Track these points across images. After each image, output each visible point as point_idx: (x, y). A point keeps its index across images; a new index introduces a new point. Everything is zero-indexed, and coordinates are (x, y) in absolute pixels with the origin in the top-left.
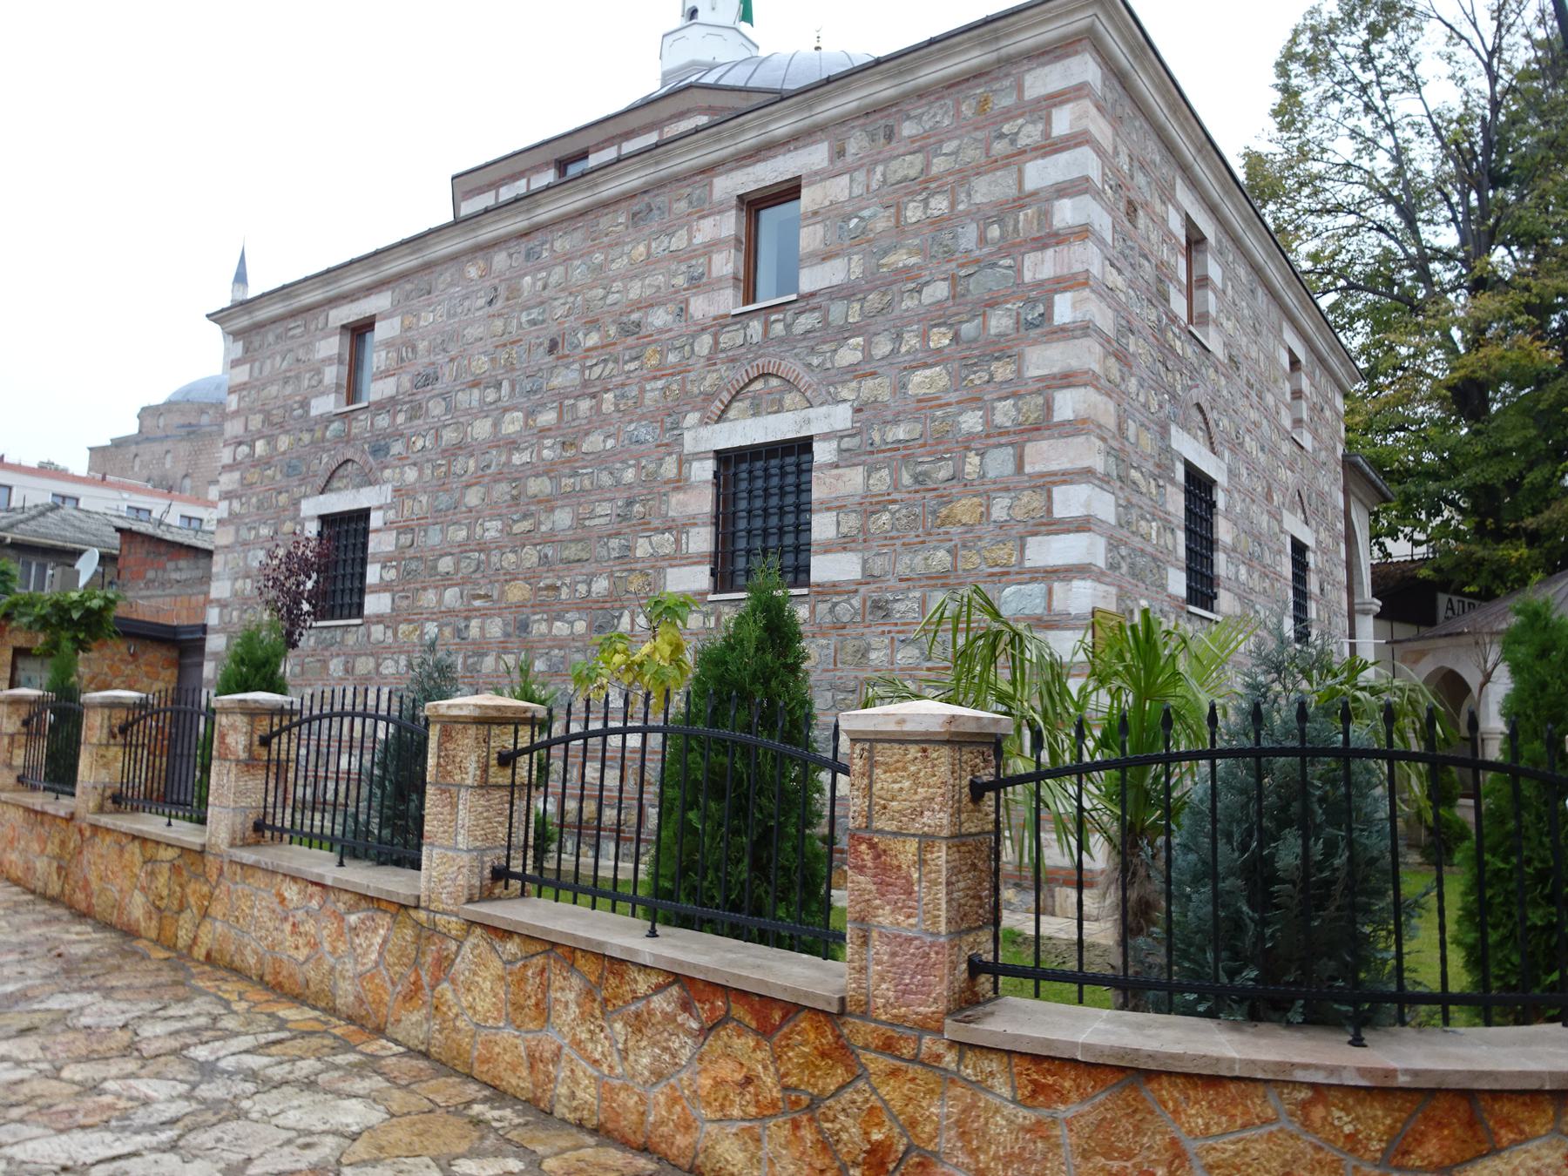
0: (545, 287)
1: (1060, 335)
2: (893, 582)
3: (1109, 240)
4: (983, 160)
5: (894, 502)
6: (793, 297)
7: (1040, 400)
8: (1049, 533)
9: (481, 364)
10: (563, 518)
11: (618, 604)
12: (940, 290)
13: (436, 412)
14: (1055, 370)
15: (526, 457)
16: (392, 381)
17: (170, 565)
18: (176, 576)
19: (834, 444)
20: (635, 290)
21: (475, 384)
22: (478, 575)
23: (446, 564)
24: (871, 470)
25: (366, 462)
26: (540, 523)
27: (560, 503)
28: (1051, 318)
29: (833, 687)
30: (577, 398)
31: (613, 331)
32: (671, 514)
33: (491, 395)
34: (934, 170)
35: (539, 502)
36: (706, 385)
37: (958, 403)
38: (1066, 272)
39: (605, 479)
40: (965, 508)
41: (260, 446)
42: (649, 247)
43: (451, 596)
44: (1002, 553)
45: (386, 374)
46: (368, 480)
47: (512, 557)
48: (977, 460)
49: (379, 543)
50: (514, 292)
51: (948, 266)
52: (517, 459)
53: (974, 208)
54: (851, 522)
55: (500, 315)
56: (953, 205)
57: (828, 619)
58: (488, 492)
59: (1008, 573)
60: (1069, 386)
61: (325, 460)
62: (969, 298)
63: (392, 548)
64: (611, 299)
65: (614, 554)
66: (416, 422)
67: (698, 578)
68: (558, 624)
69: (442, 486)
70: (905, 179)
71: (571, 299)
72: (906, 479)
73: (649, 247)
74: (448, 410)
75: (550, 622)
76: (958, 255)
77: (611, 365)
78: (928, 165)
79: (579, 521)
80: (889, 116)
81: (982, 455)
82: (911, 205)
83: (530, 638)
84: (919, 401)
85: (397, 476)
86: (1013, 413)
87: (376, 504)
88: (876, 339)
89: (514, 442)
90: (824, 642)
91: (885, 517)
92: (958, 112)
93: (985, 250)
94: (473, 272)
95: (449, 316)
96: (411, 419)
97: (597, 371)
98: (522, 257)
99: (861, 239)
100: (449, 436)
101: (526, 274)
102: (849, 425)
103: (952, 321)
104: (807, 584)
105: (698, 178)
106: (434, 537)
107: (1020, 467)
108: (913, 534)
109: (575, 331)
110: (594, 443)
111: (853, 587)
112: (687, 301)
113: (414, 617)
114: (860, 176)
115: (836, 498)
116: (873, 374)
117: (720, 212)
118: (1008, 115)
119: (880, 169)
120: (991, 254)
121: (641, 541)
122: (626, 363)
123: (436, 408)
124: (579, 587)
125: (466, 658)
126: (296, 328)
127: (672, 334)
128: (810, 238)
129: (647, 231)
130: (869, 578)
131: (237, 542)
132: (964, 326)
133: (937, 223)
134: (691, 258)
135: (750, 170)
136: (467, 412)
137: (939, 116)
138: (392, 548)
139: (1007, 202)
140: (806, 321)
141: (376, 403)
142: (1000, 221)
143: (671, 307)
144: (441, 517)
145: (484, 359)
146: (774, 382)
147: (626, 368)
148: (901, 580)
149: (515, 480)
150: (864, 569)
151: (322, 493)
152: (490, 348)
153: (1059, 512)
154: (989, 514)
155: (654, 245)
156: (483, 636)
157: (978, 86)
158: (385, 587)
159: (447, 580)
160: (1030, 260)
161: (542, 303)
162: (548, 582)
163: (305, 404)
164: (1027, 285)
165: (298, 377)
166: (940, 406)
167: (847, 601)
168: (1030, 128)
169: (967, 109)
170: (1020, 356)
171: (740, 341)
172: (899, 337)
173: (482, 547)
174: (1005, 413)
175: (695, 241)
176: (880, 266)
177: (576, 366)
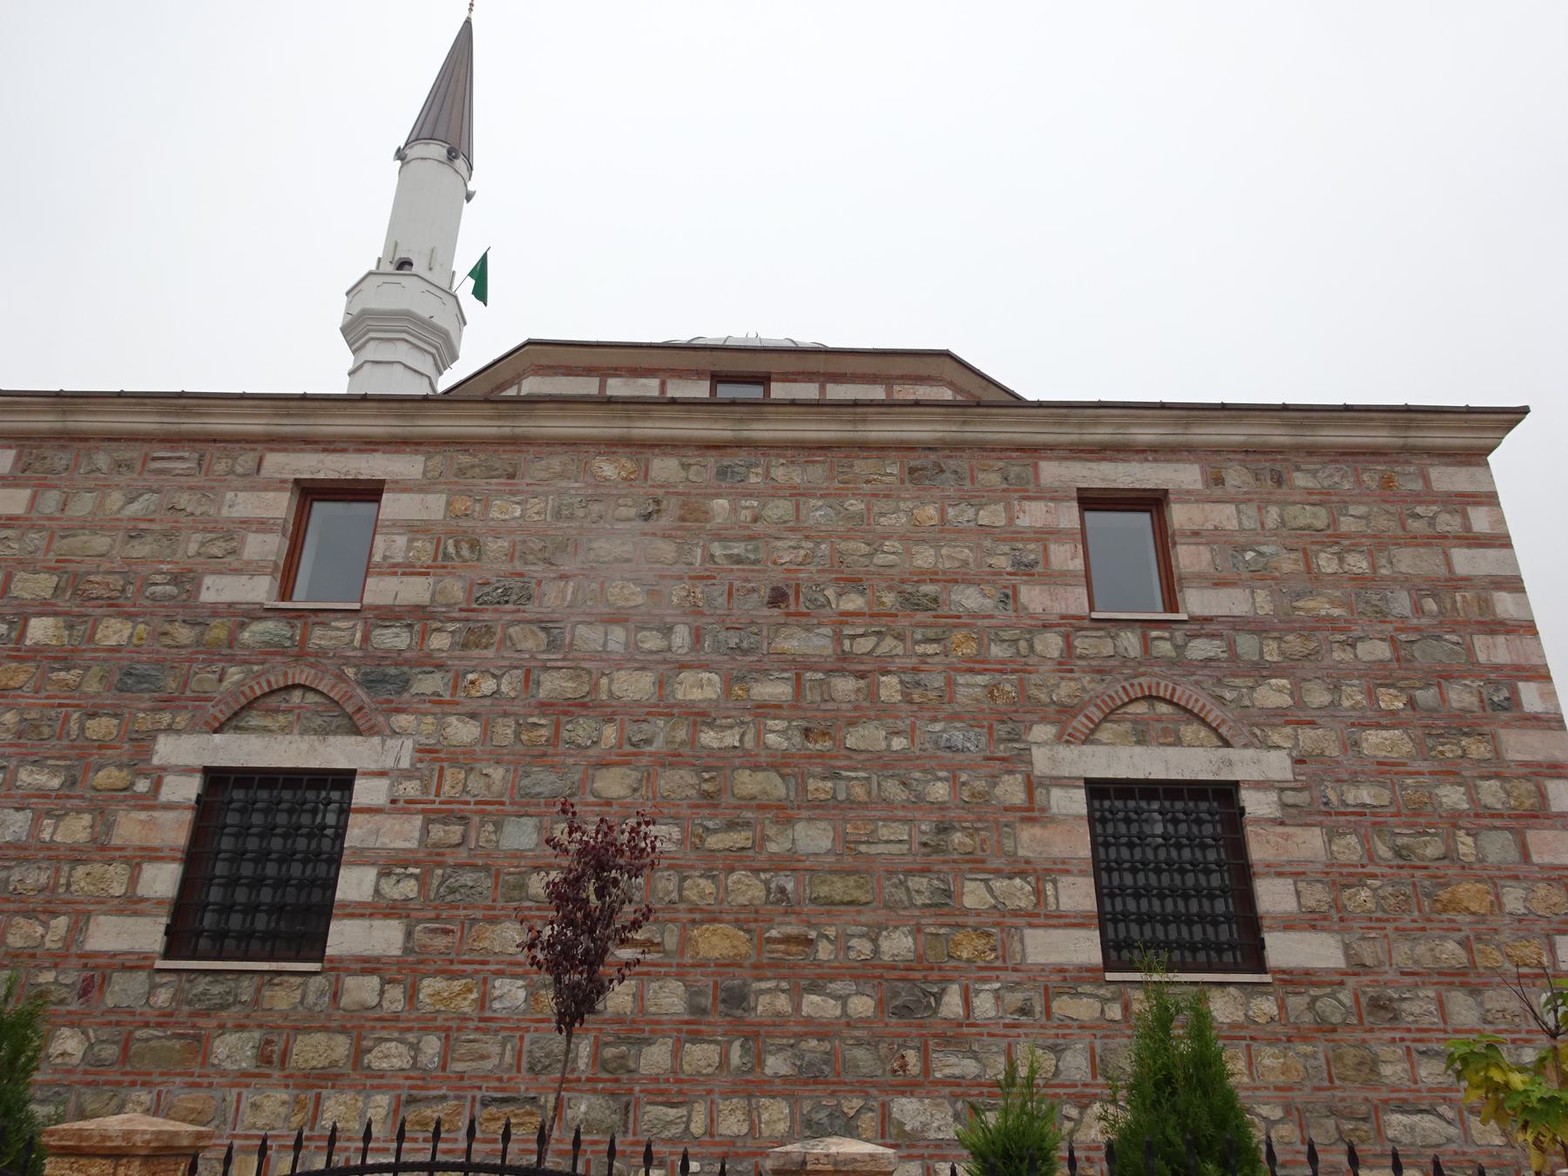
0: (755, 520)
5: (1373, 876)
9: (629, 595)
10: (814, 838)
11: (935, 975)
13: (529, 644)
14: (1539, 757)
15: (731, 738)
19: (1273, 796)
20: (925, 558)
21: (616, 618)
24: (1332, 834)
26: (766, 838)
27: (805, 813)
28: (1519, 704)
29: (1332, 1112)
30: (829, 672)
31: (889, 599)
32: (1021, 852)
33: (652, 641)
35: (762, 807)
37: (1431, 773)
38: (1523, 661)
39: (893, 790)
42: (943, 512)
47: (707, 886)
48: (1469, 840)
51: (1384, 626)
52: (709, 738)
53: (1401, 578)
54: (1317, 896)
56: (1374, 567)
58: (649, 778)
63: (413, 844)
64: (880, 559)
67: (1086, 948)
68: (815, 998)
70: (1309, 527)
72: (1383, 851)
73: (943, 512)
74: (552, 645)
75: (796, 994)
76: (1390, 618)
79: (847, 844)
81: (1473, 834)
82: (1322, 555)
83: (751, 1017)
84: (1379, 763)
86: (1502, 795)
87: (373, 767)
88: (1308, 685)
89: (703, 714)
90: (1309, 1049)
91: (1364, 894)
93: (1424, 621)
95: (558, 515)
96: (465, 646)
97: (864, 645)
100: (553, 685)
101: (718, 496)
103: (1401, 684)
105: (1014, 454)
108: (1406, 917)
111: (1337, 978)
112: (1014, 586)
114: (1250, 510)
115: (1290, 863)
116: (1311, 723)
117: (1052, 499)
118: (1418, 498)
119: (1274, 511)
120: (1434, 627)
121: (969, 886)
122: (917, 642)
124: (854, 942)
125: (597, 1046)
126: (183, 462)
127: (993, 622)
129: (937, 493)
130: (1357, 967)
133: (1357, 578)
134: (1013, 539)
135: (1093, 465)
136: (593, 656)
137: (1339, 478)
140: (1200, 649)
141: (378, 607)
146: (1163, 708)
147: (920, 649)
148: (1403, 973)
149: (707, 769)
150: (1347, 956)
151: (216, 731)
154: (1501, 905)
155: (951, 512)
156: (642, 1010)
160: (1480, 642)
161: (751, 538)
163: (187, 579)
165: (170, 535)
166: (1410, 774)
167: (1332, 995)
169: (1370, 480)
172: (1336, 688)
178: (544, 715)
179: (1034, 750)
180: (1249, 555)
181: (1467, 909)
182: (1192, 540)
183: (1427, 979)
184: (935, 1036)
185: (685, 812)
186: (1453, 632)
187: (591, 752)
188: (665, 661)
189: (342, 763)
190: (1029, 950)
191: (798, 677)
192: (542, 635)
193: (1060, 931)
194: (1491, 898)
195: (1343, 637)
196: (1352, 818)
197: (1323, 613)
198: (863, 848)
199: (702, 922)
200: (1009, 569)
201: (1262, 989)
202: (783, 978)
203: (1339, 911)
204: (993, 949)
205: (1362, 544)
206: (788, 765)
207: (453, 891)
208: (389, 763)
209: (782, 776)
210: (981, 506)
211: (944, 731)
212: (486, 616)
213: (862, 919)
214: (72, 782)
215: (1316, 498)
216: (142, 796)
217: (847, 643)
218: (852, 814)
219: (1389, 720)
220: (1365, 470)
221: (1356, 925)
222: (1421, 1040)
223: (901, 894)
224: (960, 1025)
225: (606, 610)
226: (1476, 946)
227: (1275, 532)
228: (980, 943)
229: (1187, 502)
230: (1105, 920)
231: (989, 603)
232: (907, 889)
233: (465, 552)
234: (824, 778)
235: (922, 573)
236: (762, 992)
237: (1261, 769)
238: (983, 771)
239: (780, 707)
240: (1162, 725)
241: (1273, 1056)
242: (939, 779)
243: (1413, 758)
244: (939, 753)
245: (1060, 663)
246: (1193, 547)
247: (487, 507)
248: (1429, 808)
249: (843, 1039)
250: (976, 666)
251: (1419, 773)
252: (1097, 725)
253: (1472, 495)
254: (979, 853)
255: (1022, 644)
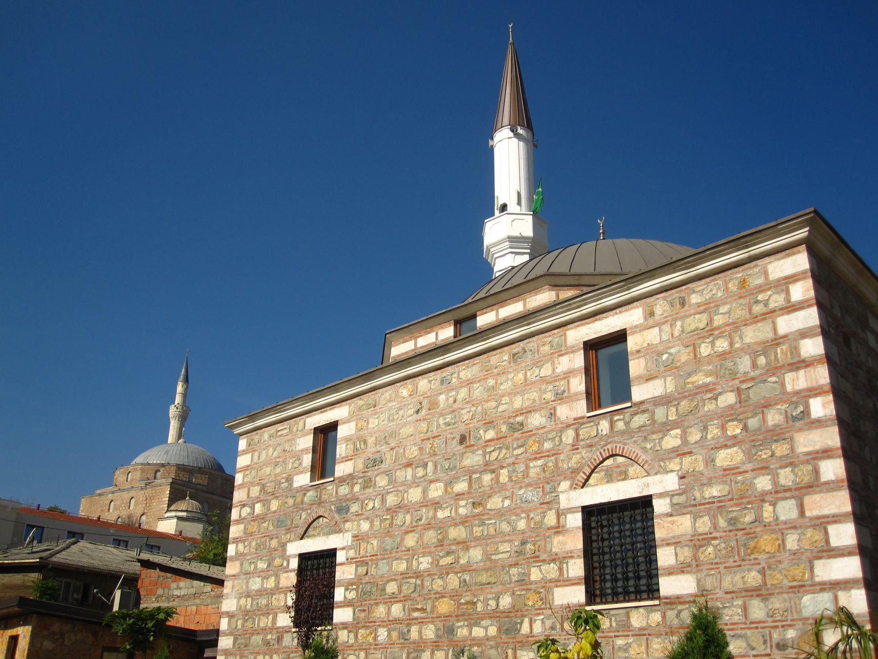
0: (455, 401)
1: (817, 424)
2: (721, 594)
3: (838, 361)
4: (748, 316)
5: (715, 538)
6: (629, 404)
7: (810, 467)
8: (830, 557)
9: (412, 452)
10: (476, 554)
12: (729, 399)
14: (817, 447)
15: (447, 513)
16: (350, 463)
17: (174, 585)
18: (176, 593)
19: (668, 500)
21: (409, 465)
22: (415, 595)
23: (392, 588)
25: (333, 518)
26: (459, 558)
27: (473, 544)
28: (809, 414)
30: (481, 472)
31: (504, 428)
32: (554, 550)
33: (420, 472)
34: (716, 324)
35: (458, 543)
36: (573, 463)
37: (753, 470)
38: (814, 384)
40: (766, 542)
41: (258, 508)
43: (397, 610)
44: (797, 572)
45: (347, 459)
46: (336, 529)
47: (440, 582)
48: (771, 508)
49: (344, 573)
50: (434, 404)
51: (733, 382)
52: (441, 514)
54: (686, 553)
55: (424, 420)
56: (731, 344)
57: (676, 622)
58: (421, 536)
59: (803, 586)
60: (829, 457)
61: (304, 517)
62: (751, 402)
63: (353, 576)
65: (515, 579)
66: (367, 491)
69: (388, 533)
71: (473, 409)
72: (722, 523)
73: (526, 374)
75: (470, 627)
76: (739, 375)
77: (504, 451)
78: (711, 321)
79: (487, 556)
80: (681, 291)
81: (774, 505)
82: (703, 345)
83: (455, 638)
84: (725, 470)
85: (355, 527)
86: (792, 477)
88: (690, 430)
89: (438, 503)
91: (710, 549)
92: (727, 288)
93: (757, 372)
94: (404, 391)
95: (389, 421)
96: (364, 488)
97: (495, 455)
98: (438, 383)
99: (671, 367)
100: (391, 500)
101: (441, 393)
102: (677, 487)
103: (741, 417)
104: (659, 598)
105: (556, 331)
106: (383, 568)
107: (802, 513)
108: (731, 560)
109: (478, 429)
110: (495, 503)
112: (555, 408)
113: (371, 624)
114: (666, 328)
115: (673, 537)
116: (690, 453)
117: (573, 352)
118: (760, 289)
119: (679, 323)
120: (762, 375)
121: (533, 570)
122: (515, 449)
123: (382, 481)
124: (490, 602)
125: (408, 654)
128: (636, 367)
129: (523, 365)
131: (241, 572)
132: (749, 421)
133: (723, 355)
134: (555, 381)
135: (591, 326)
136: (403, 484)
138: (353, 576)
139: (768, 342)
140: (639, 420)
141: (339, 478)
142: (765, 353)
143: (543, 412)
144: (385, 554)
145: (414, 448)
146: (620, 460)
147: (515, 452)
148: (727, 593)
149: (440, 528)
150: (698, 585)
151: (302, 539)
152: (419, 441)
153: (834, 542)
155: (529, 373)
156: (421, 637)
157: (739, 272)
158: (347, 603)
159: (394, 599)
160: (789, 377)
161: (453, 411)
162: (468, 599)
163: (290, 480)
164: (789, 394)
166: (740, 473)
168: (775, 297)
169: (733, 286)
170: (792, 439)
171: (594, 433)
172: (705, 428)
173: (418, 575)
174: (786, 477)
175: (557, 370)
176: (686, 384)
177: (480, 452)
178: (388, 514)
179: (561, 495)
180: (665, 357)
181: (764, 550)
182: (637, 355)
183: (738, 595)
184: (519, 642)
185: (433, 549)
186: (774, 374)
187: (403, 528)
188: (425, 481)
189: (332, 546)
190: (555, 598)
191: (470, 477)
192: (387, 478)
193: (569, 588)
194: (780, 542)
195: (711, 395)
196: (707, 506)
197: (701, 382)
198: (493, 557)
199: (440, 598)
200: (553, 398)
201: (656, 608)
202: (465, 620)
203: (696, 561)
204: (542, 600)
205: (725, 331)
206: (466, 522)
207: (365, 594)
208: (345, 544)
209: (465, 527)
210: (542, 366)
211: (525, 493)
212: (369, 474)
213: (493, 590)
214: (269, 565)
215: (702, 308)
216: (284, 568)
217: (488, 456)
218: (489, 541)
219: (734, 441)
220: (732, 279)
221: (704, 568)
222: (732, 630)
223: (507, 578)
224: (528, 637)
225: (405, 461)
226: (768, 573)
227: (679, 338)
228: (536, 597)
229: (635, 332)
230: (589, 581)
231: (544, 420)
232: (510, 575)
233: (362, 446)
234: (479, 526)
235: (517, 411)
236: (459, 627)
237: (659, 485)
238: (540, 511)
239: (463, 494)
240: (618, 470)
241: (659, 643)
242: (522, 518)
243: (744, 463)
244: (523, 505)
245: (573, 446)
246: (636, 361)
247: (368, 423)
248: (750, 492)
249: (486, 646)
250: (538, 456)
251: (746, 472)
252: (589, 477)
253: (793, 276)
254: (537, 553)
255: (557, 439)
